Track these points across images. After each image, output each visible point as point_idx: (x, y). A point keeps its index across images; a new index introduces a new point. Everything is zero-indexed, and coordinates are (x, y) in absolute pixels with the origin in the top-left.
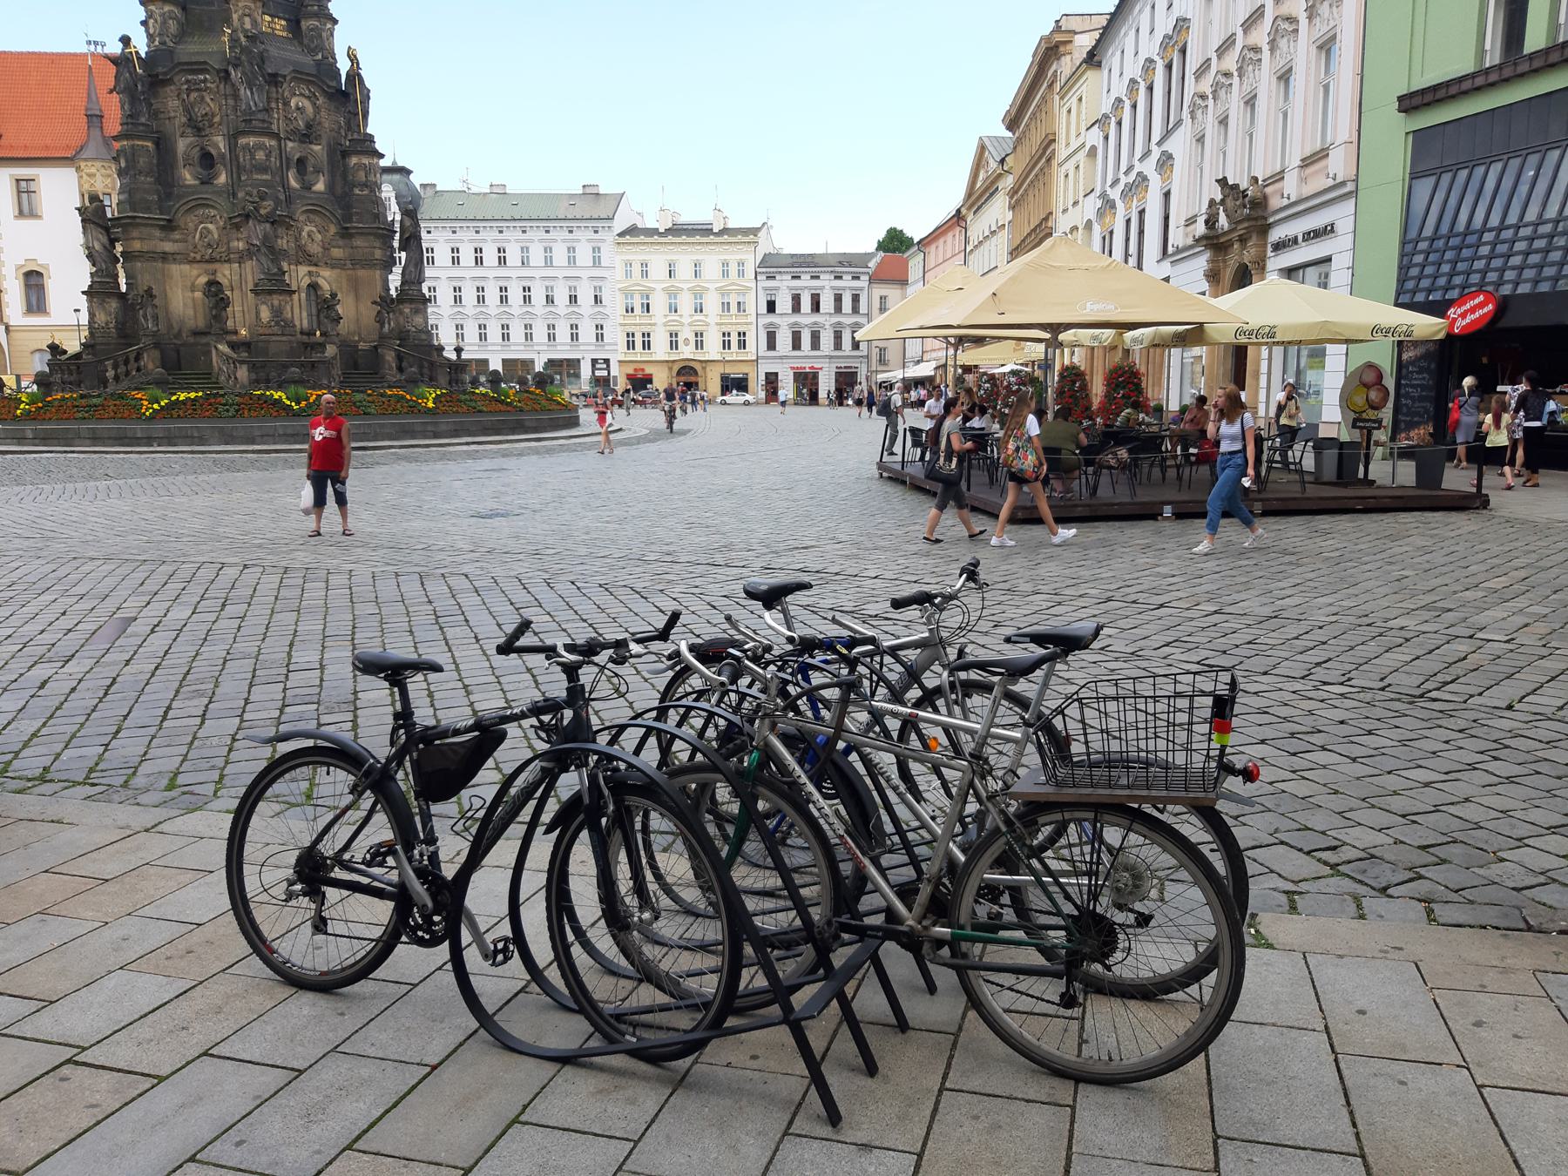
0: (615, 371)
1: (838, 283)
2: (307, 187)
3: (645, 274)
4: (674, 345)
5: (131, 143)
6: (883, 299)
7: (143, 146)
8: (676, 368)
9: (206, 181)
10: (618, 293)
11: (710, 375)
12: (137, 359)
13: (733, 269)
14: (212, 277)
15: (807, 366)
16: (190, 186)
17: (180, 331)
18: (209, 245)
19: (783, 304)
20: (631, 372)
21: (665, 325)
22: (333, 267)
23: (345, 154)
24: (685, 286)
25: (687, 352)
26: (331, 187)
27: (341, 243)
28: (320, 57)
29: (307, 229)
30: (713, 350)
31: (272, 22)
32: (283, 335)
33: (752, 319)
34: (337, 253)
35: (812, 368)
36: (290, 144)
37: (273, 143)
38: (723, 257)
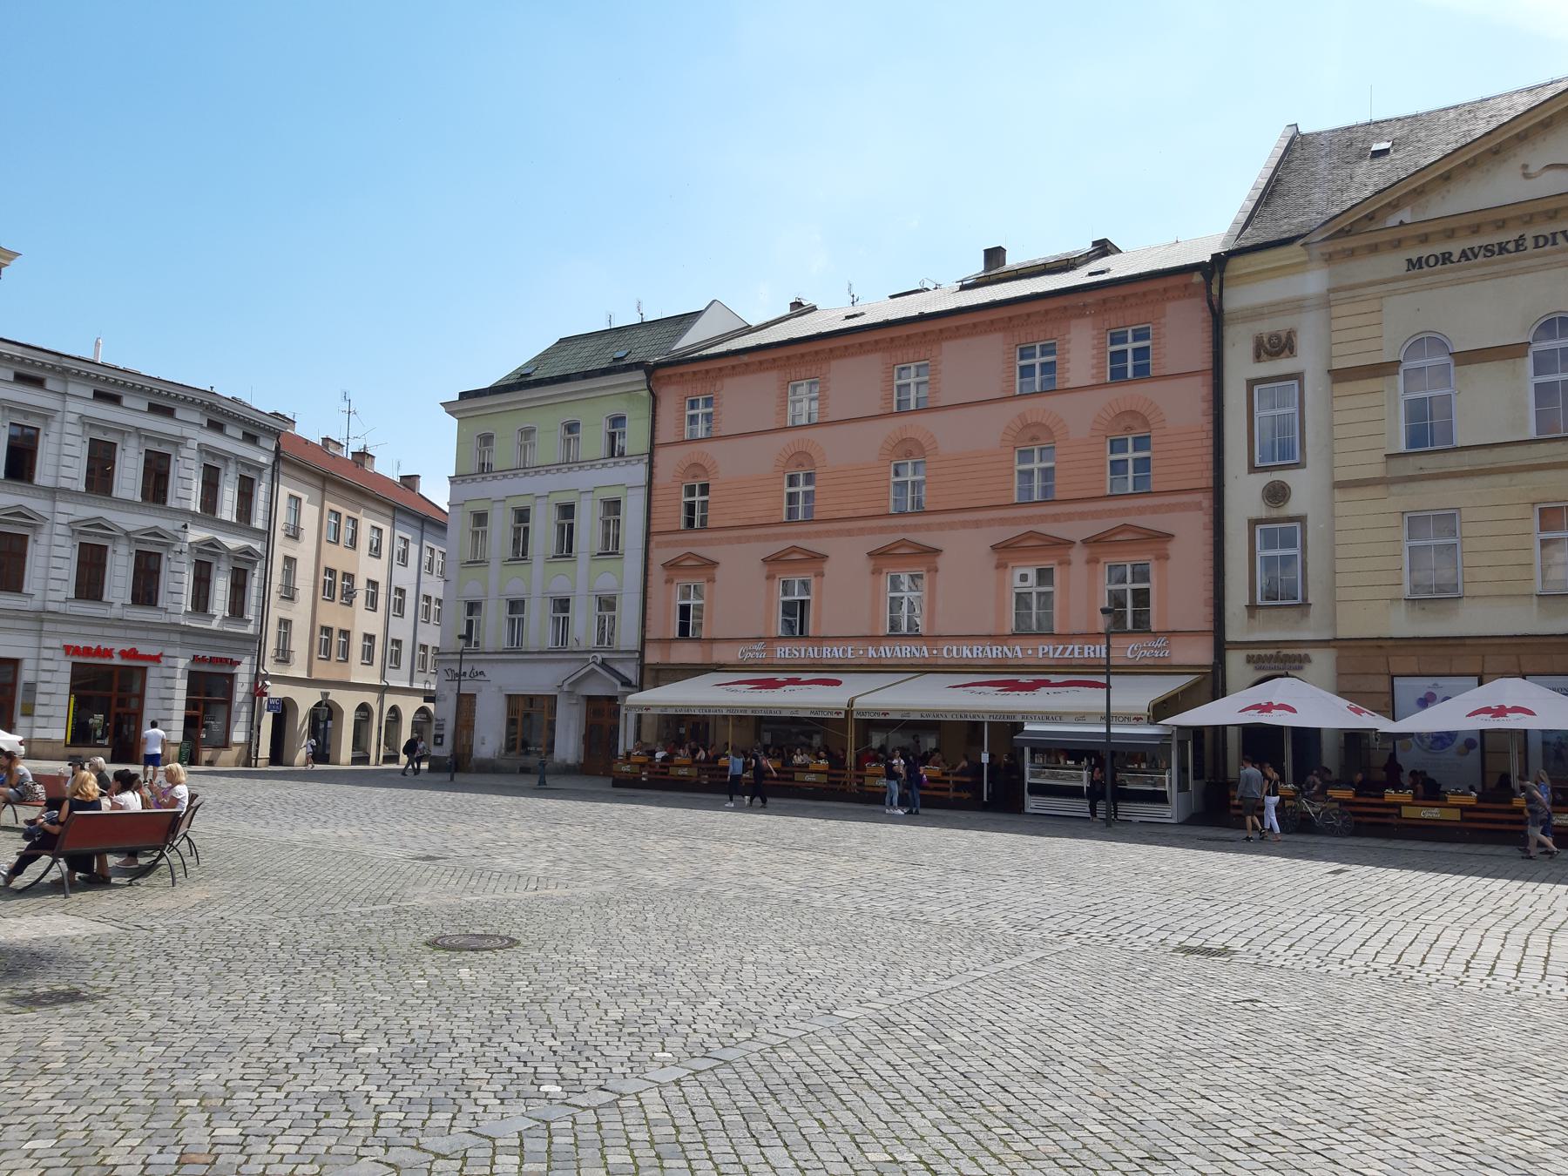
15: (118, 647)
35: (132, 654)
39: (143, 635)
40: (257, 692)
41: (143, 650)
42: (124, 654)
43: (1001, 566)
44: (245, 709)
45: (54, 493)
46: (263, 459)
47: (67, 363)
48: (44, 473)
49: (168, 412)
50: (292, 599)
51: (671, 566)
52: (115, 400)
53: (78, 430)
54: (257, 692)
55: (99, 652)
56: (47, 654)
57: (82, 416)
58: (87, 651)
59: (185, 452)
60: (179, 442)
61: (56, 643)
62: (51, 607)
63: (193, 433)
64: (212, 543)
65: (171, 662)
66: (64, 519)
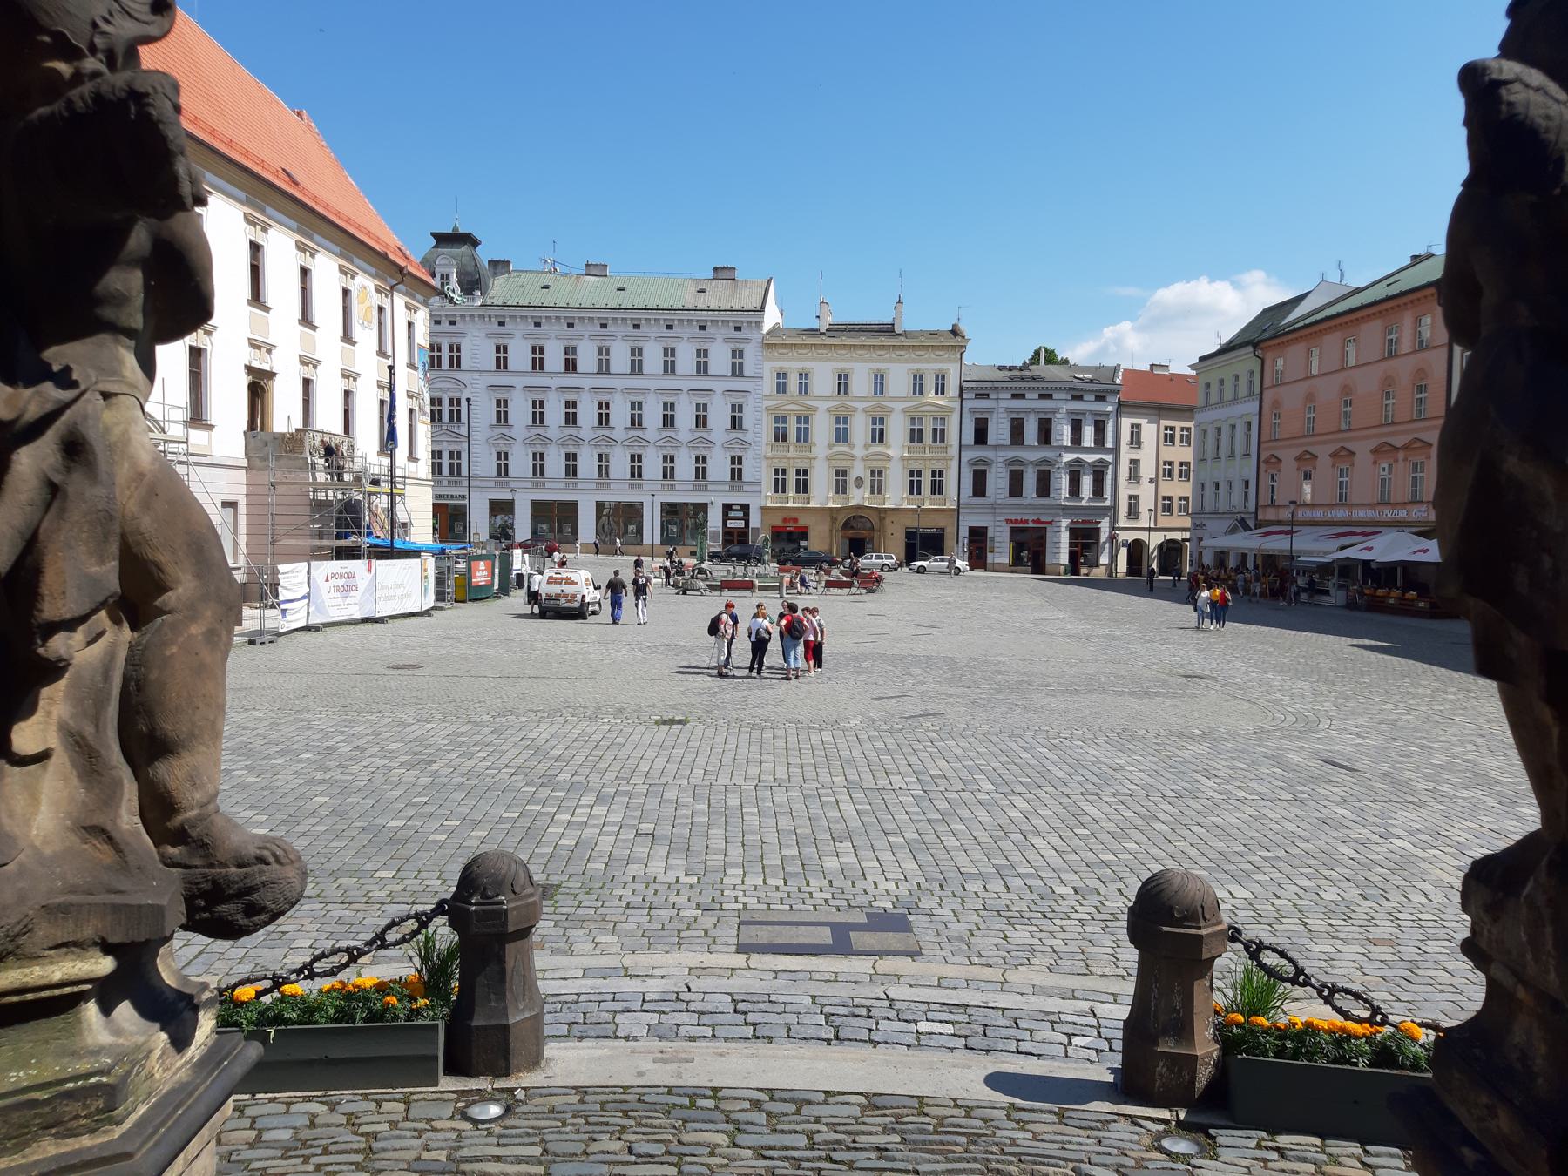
0: (755, 521)
1: (1078, 406)
3: (805, 388)
4: (841, 488)
6: (1136, 428)
8: (842, 519)
10: (765, 414)
11: (890, 528)
13: (929, 384)
15: (1031, 518)
19: (999, 431)
20: (778, 522)
21: (829, 459)
24: (860, 405)
25: (859, 497)
30: (895, 496)
33: (954, 451)
35: (1038, 521)
38: (915, 366)
39: (1042, 511)
40: (1112, 538)
41: (1043, 519)
42: (1034, 521)
43: (1375, 462)
44: (1107, 545)
45: (996, 447)
46: (1110, 408)
47: (996, 385)
48: (991, 440)
49: (1049, 397)
50: (1138, 483)
51: (1266, 462)
52: (1022, 396)
53: (1005, 415)
54: (1112, 538)
55: (1022, 521)
56: (998, 524)
57: (1007, 408)
58: (1016, 521)
59: (1058, 416)
60: (1055, 411)
61: (1002, 518)
62: (999, 502)
63: (1063, 407)
64: (1078, 460)
65: (1058, 524)
66: (1001, 460)
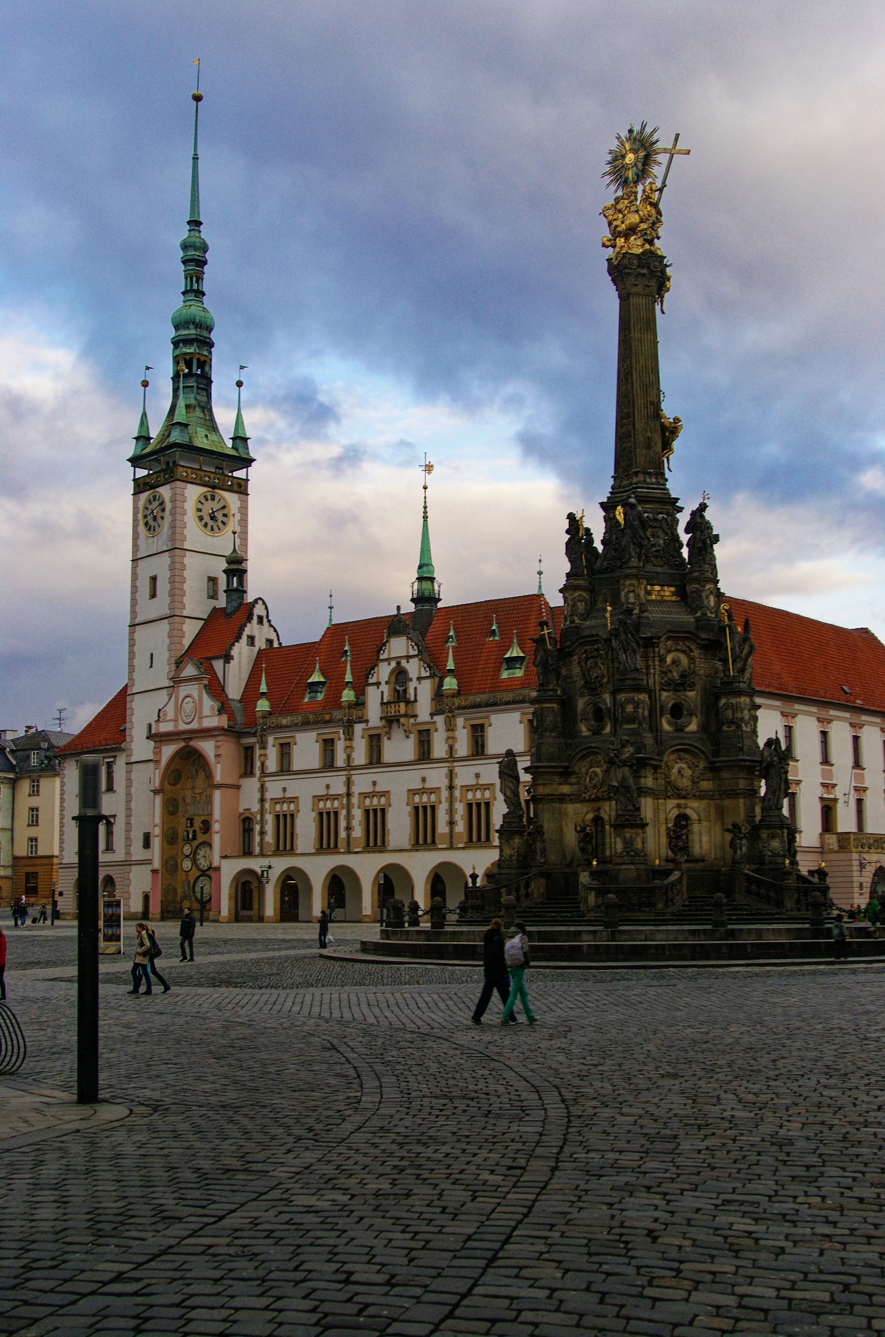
2: (680, 729)
5: (541, 705)
7: (549, 708)
9: (597, 732)
12: (527, 886)
14: (597, 813)
16: (585, 737)
17: (571, 862)
18: (595, 786)
22: (701, 798)
23: (718, 698)
26: (704, 728)
27: (710, 775)
28: (699, 614)
29: (677, 766)
31: (662, 590)
32: (632, 864)
34: (706, 785)
36: (665, 694)
37: (644, 697)
